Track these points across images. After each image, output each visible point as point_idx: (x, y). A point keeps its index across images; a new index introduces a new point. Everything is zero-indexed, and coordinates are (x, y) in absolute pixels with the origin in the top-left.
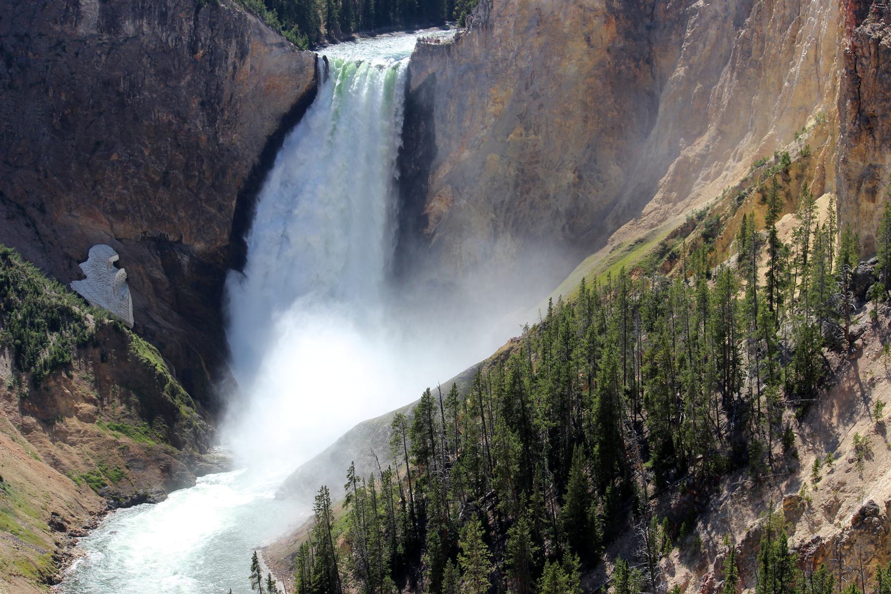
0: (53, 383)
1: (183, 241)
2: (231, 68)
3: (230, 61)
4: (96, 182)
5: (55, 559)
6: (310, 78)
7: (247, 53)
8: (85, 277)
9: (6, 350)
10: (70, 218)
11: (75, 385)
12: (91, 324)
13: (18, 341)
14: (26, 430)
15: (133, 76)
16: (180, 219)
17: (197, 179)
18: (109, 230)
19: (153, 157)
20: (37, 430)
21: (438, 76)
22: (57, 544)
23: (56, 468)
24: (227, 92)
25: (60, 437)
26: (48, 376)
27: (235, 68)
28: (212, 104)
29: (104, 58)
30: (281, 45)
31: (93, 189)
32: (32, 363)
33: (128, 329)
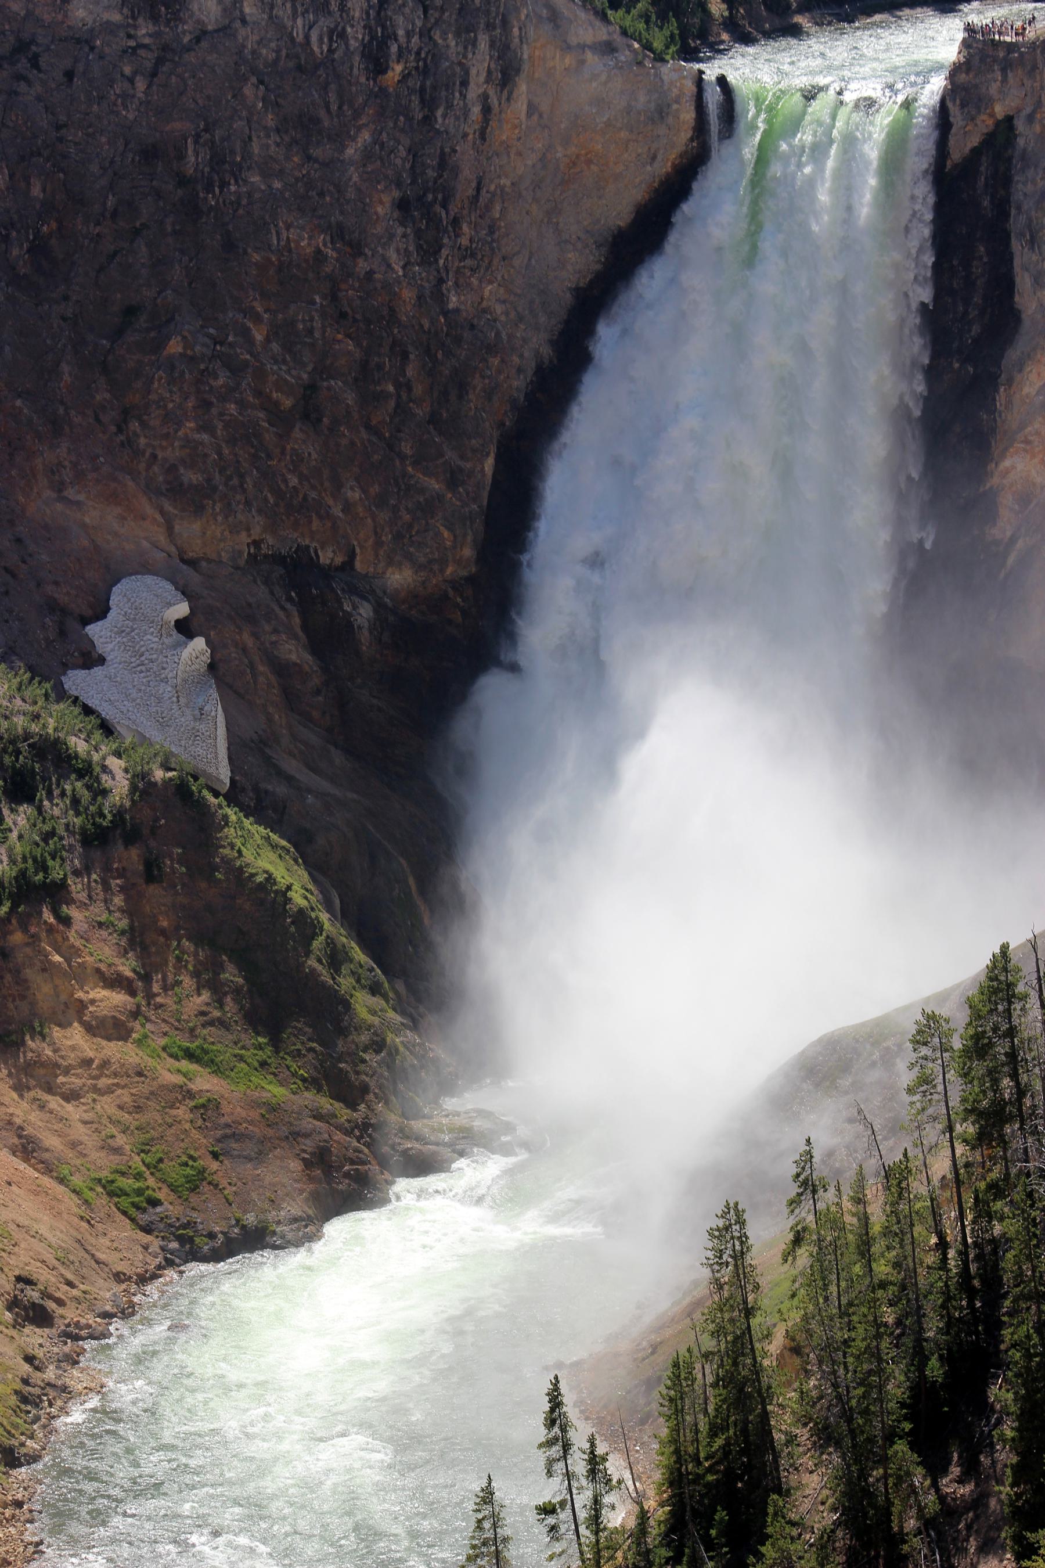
0: (18, 938)
1: (358, 565)
2: (476, 110)
3: (473, 92)
4: (126, 414)
5: (25, 1399)
6: (685, 135)
7: (518, 71)
8: (101, 661)
10: (59, 507)
11: (78, 943)
12: (118, 784)
15: (218, 134)
16: (347, 508)
17: (392, 403)
18: (162, 539)
19: (275, 347)
21: (1020, 125)
22: (29, 1359)
23: (26, 1160)
24: (467, 172)
27: (487, 110)
28: (429, 206)
29: (141, 84)
30: (608, 48)
31: (120, 430)
33: (216, 794)
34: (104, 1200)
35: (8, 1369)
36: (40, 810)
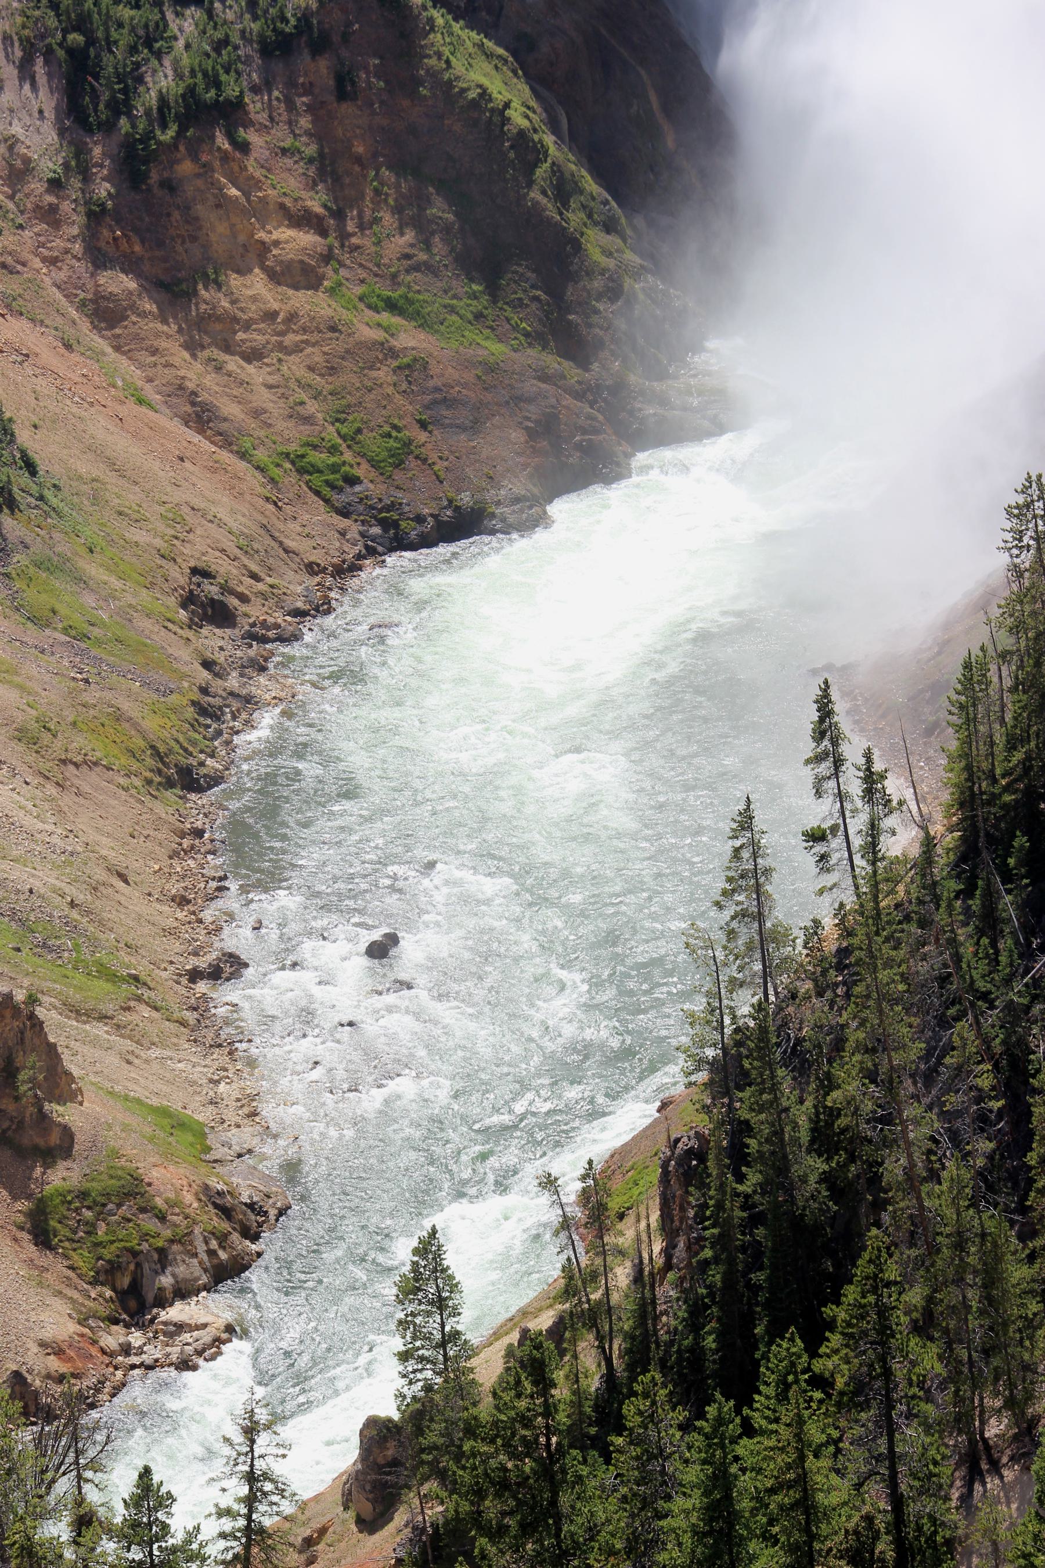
0: (186, 167)
9: (39, 67)
11: (258, 173)
13: (76, 38)
14: (106, 314)
20: (143, 315)
23: (201, 431)
25: (211, 333)
26: (174, 145)
32: (121, 106)
34: (294, 477)
35: (184, 676)
36: (210, 13)
